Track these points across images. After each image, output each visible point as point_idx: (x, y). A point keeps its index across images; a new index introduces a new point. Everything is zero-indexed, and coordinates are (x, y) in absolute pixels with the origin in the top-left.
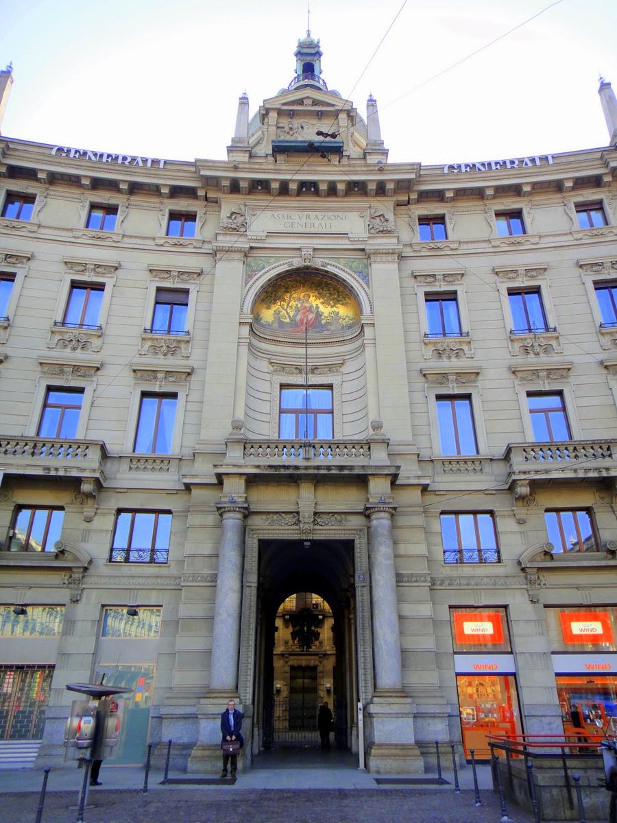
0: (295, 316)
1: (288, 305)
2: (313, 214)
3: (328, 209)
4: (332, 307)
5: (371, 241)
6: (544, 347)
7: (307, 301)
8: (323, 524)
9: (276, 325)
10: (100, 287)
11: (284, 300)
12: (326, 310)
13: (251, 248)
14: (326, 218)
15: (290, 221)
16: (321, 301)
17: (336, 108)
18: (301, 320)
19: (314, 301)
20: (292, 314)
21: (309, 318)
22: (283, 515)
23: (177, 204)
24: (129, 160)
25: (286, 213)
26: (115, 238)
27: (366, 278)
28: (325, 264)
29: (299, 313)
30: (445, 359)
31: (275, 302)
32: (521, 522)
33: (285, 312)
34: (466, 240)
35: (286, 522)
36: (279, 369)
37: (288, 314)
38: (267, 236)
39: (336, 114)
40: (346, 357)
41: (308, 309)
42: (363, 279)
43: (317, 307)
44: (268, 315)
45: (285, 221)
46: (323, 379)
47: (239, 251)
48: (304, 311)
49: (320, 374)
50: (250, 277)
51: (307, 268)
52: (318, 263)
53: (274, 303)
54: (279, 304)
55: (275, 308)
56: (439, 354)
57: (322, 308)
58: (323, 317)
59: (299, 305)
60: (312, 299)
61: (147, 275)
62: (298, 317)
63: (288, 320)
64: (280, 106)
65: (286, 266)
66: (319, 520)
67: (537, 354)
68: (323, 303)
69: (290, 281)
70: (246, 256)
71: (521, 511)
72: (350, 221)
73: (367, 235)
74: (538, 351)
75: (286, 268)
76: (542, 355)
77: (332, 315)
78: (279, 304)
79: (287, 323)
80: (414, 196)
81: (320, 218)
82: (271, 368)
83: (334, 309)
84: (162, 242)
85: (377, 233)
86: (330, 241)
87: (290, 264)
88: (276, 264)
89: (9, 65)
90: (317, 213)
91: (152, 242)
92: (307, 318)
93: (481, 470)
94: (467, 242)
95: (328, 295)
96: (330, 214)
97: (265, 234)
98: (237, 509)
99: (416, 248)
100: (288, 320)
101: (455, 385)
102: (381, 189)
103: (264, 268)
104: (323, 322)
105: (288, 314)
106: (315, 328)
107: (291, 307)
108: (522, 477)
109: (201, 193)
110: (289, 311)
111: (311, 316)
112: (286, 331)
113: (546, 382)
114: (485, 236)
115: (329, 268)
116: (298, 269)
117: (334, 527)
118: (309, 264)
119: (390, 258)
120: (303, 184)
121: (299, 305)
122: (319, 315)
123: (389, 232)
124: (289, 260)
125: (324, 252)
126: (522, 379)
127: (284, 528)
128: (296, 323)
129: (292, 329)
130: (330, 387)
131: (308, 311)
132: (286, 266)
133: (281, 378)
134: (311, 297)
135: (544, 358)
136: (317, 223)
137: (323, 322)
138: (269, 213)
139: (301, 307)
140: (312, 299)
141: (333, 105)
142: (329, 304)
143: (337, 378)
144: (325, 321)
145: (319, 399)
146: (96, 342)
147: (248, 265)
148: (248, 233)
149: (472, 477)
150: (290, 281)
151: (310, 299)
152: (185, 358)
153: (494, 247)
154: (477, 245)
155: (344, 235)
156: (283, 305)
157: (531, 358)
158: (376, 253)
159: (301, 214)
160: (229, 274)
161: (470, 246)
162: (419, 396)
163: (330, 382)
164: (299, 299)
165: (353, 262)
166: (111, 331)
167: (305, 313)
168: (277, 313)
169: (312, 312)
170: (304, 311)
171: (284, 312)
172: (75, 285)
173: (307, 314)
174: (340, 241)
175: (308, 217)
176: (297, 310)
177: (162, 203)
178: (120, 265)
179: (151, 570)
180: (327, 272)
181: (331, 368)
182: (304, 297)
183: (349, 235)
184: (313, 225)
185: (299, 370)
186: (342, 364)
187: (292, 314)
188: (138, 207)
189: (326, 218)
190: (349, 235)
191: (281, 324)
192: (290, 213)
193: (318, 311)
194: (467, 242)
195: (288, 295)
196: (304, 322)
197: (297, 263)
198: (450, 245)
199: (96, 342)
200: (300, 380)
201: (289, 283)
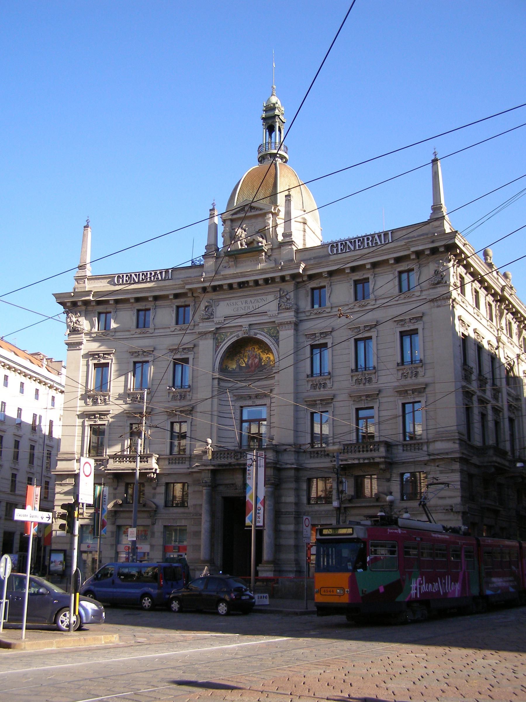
0: (248, 361)
2: (249, 300)
5: (280, 316)
7: (254, 352)
9: (238, 369)
11: (241, 353)
12: (264, 356)
13: (217, 329)
14: (256, 301)
15: (237, 306)
17: (263, 211)
18: (252, 364)
20: (246, 360)
25: (234, 301)
26: (151, 331)
28: (256, 334)
30: (318, 390)
39: (265, 214)
43: (259, 355)
45: (235, 306)
47: (210, 332)
50: (218, 347)
52: (252, 334)
56: (314, 387)
60: (256, 350)
62: (250, 362)
63: (244, 365)
64: (230, 217)
65: (236, 337)
68: (262, 352)
70: (215, 334)
72: (268, 303)
73: (277, 312)
75: (235, 339)
80: (305, 278)
81: (253, 301)
82: (235, 398)
83: (268, 355)
84: (173, 329)
86: (258, 318)
87: (238, 336)
88: (231, 336)
90: (251, 299)
96: (258, 298)
99: (308, 314)
100: (244, 365)
102: (283, 279)
103: (224, 340)
104: (263, 364)
106: (259, 368)
111: (257, 360)
115: (259, 336)
118: (247, 335)
122: (261, 359)
123: (289, 309)
124: (236, 334)
125: (255, 326)
132: (236, 337)
135: (368, 386)
136: (251, 305)
137: (263, 364)
140: (256, 350)
141: (261, 209)
142: (265, 352)
147: (217, 339)
148: (214, 319)
157: (361, 386)
158: (281, 324)
159: (243, 300)
160: (206, 346)
164: (249, 351)
165: (271, 330)
174: (264, 318)
175: (246, 302)
178: (155, 348)
179: (181, 510)
184: (249, 308)
187: (246, 360)
188: (161, 307)
189: (256, 301)
190: (268, 313)
191: (241, 368)
192: (237, 301)
197: (241, 335)
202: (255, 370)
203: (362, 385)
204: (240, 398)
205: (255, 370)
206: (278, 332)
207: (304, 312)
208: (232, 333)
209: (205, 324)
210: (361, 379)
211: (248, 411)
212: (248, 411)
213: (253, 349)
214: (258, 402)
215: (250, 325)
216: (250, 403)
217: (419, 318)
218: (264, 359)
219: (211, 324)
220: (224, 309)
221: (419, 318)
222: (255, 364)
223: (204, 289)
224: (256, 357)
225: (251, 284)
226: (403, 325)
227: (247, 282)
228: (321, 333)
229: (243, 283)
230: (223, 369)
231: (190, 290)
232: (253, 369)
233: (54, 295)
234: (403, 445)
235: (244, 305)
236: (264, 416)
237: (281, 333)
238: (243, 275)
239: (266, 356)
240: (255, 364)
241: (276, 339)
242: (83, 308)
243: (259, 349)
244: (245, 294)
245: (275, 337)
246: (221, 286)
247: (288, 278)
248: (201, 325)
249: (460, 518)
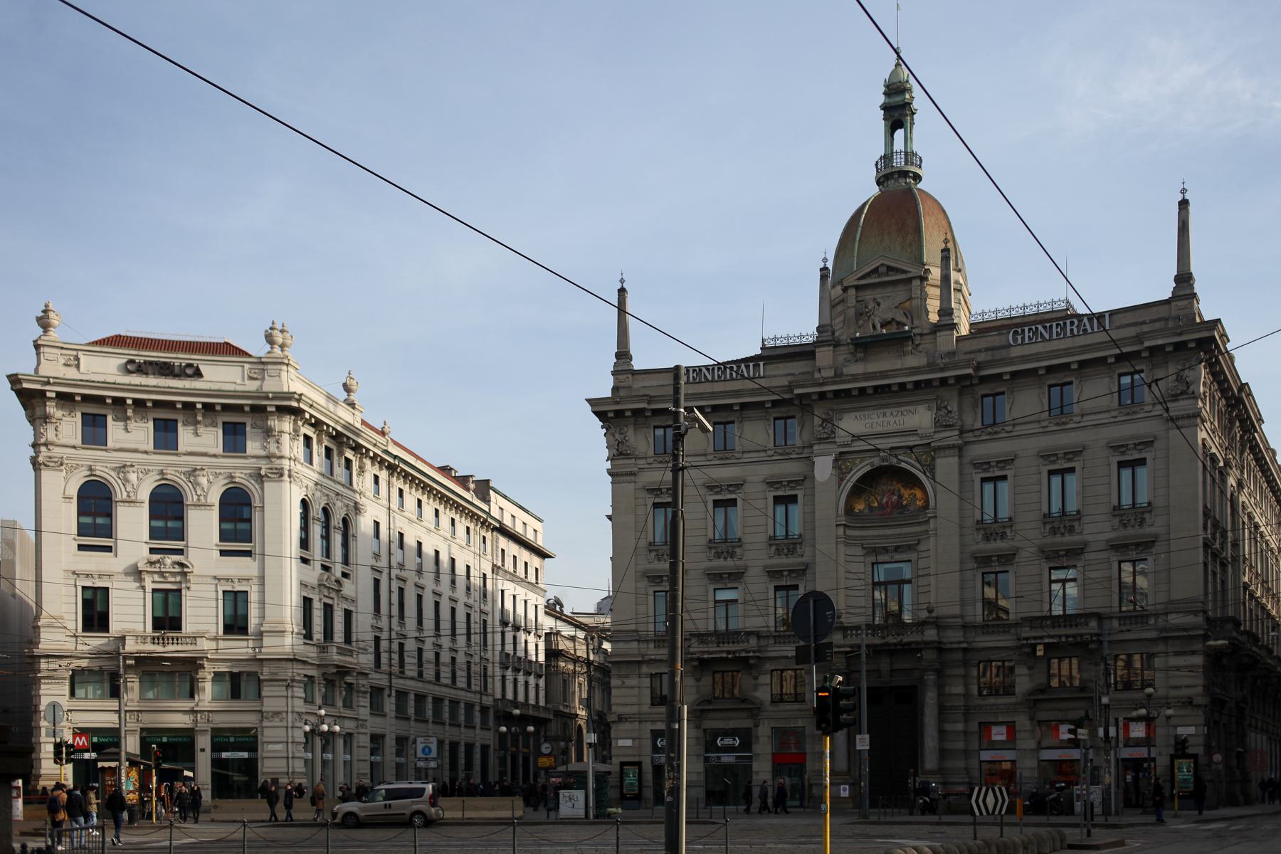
2: (888, 411)
3: (899, 405)
5: (937, 436)
9: (866, 511)
10: (733, 502)
12: (906, 493)
19: (897, 486)
44: (859, 507)
50: (841, 480)
51: (886, 467)
57: (903, 491)
61: (764, 487)
72: (920, 418)
75: (868, 468)
86: (903, 439)
87: (872, 464)
91: (762, 454)
109: (797, 402)
111: (895, 498)
115: (903, 465)
116: (881, 467)
119: (952, 452)
120: (876, 388)
122: (900, 497)
136: (892, 419)
138: (852, 415)
146: (738, 551)
147: (840, 468)
155: (913, 432)
158: (940, 448)
161: (1023, 427)
166: (747, 539)
172: (717, 503)
174: (912, 438)
175: (885, 415)
184: (888, 423)
191: (871, 509)
197: (877, 462)
199: (738, 551)
204: (874, 551)
206: (933, 459)
207: (972, 431)
208: (862, 460)
209: (822, 446)
211: (886, 570)
212: (886, 570)
214: (898, 557)
215: (892, 449)
216: (886, 558)
217: (1149, 444)
219: (828, 446)
220: (852, 424)
221: (1149, 444)
223: (822, 395)
225: (895, 388)
226: (1123, 453)
228: (998, 462)
229: (882, 387)
230: (849, 510)
231: (800, 396)
233: (588, 400)
234: (1120, 618)
235: (881, 419)
236: (908, 577)
237: (938, 461)
238: (883, 374)
239: (909, 492)
241: (930, 469)
242: (632, 420)
244: (883, 402)
246: (847, 392)
247: (952, 381)
248: (815, 447)
249: (1200, 713)
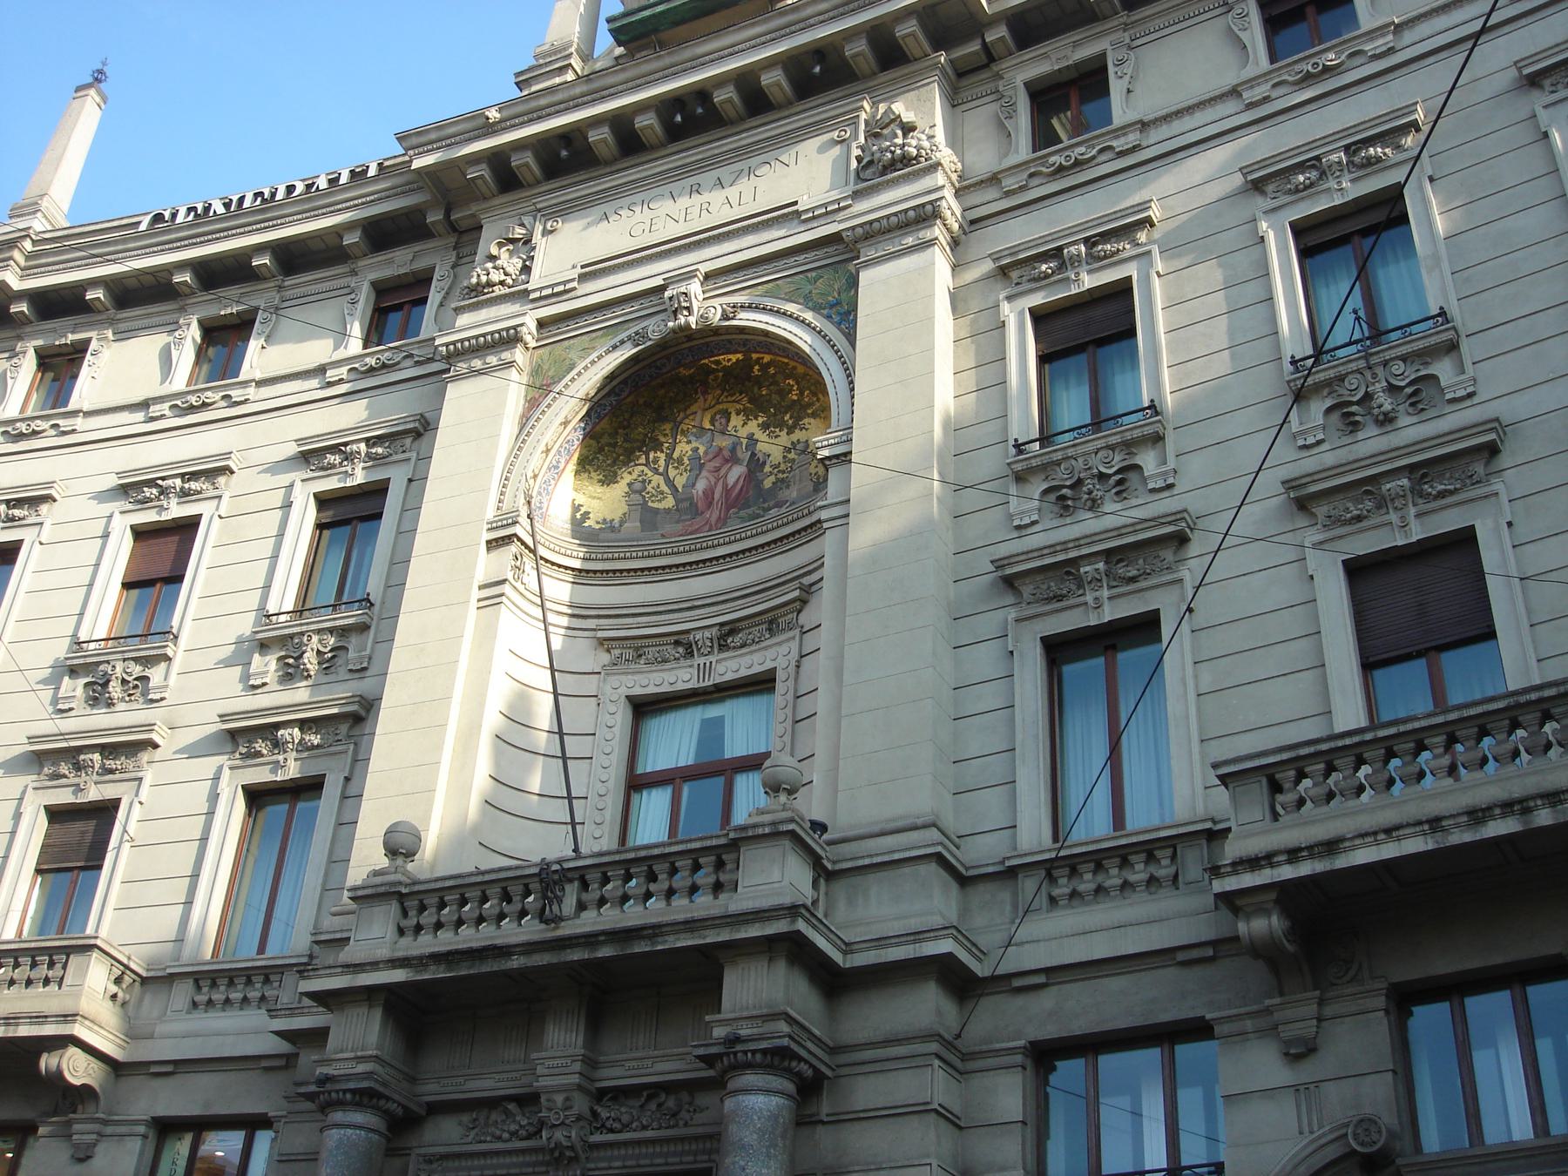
1: (669, 457)
4: (790, 432)
6: (1409, 390)
8: (617, 1125)
11: (658, 446)
12: (772, 447)
16: (760, 420)
18: (709, 494)
19: (744, 428)
21: (731, 480)
22: (512, 1106)
23: (391, 262)
24: (300, 188)
27: (844, 314)
29: (704, 473)
31: (628, 458)
32: (1300, 1052)
33: (661, 479)
34: (1164, 112)
35: (513, 1127)
36: (630, 653)
37: (670, 483)
38: (583, 278)
40: (806, 581)
41: (726, 453)
42: (838, 325)
46: (757, 658)
48: (716, 463)
49: (743, 646)
53: (626, 464)
54: (643, 460)
55: (626, 478)
58: (767, 469)
59: (702, 450)
60: (736, 421)
62: (701, 485)
63: (669, 502)
66: (604, 1114)
67: (1386, 420)
68: (764, 426)
69: (662, 386)
71: (1299, 1014)
74: (1387, 407)
76: (1403, 420)
77: (792, 455)
78: (643, 460)
79: (667, 511)
82: (605, 658)
83: (798, 435)
85: (883, 174)
89: (100, 67)
92: (725, 485)
93: (1176, 876)
94: (1166, 118)
95: (775, 398)
97: (575, 274)
98: (348, 1096)
100: (669, 502)
101: (1106, 593)
104: (768, 483)
105: (670, 483)
106: (746, 506)
107: (680, 461)
108: (1248, 880)
110: (672, 473)
111: (736, 473)
112: (663, 536)
113: (1412, 511)
114: (1229, 80)
115: (746, 319)
117: (649, 1134)
120: (669, 105)
121: (702, 450)
122: (756, 464)
124: (631, 331)
126: (1334, 521)
127: (509, 1146)
128: (693, 505)
129: (680, 526)
130: (762, 684)
131: (727, 461)
132: (629, 345)
133: (629, 680)
134: (733, 416)
135: (1411, 430)
137: (768, 483)
139: (706, 453)
140: (736, 421)
143: (784, 649)
144: (772, 478)
145: (744, 728)
149: (1139, 907)
150: (662, 386)
151: (732, 424)
152: (357, 675)
153: (1251, 106)
154: (1199, 118)
156: (656, 461)
157: (1371, 441)
158: (874, 232)
161: (1177, 126)
162: (985, 660)
163: (768, 665)
167: (718, 470)
168: (637, 488)
169: (737, 461)
170: (716, 463)
171: (658, 480)
173: (723, 471)
176: (697, 464)
177: (354, 273)
180: (742, 330)
181: (772, 622)
182: (712, 422)
183: (799, 207)
185: (685, 645)
186: (804, 602)
187: (680, 482)
193: (753, 454)
194: (1166, 118)
195: (667, 427)
196: (717, 496)
198: (1114, 143)
200: (682, 677)
201: (662, 392)
202: (722, 521)
203: (1371, 430)
205: (722, 521)
210: (1368, 397)
213: (720, 420)
218: (776, 454)
222: (727, 491)
224: (733, 459)
227: (701, 94)
232: (714, 515)
239: (784, 439)
240: (727, 491)
243: (748, 414)
245: (838, 303)
